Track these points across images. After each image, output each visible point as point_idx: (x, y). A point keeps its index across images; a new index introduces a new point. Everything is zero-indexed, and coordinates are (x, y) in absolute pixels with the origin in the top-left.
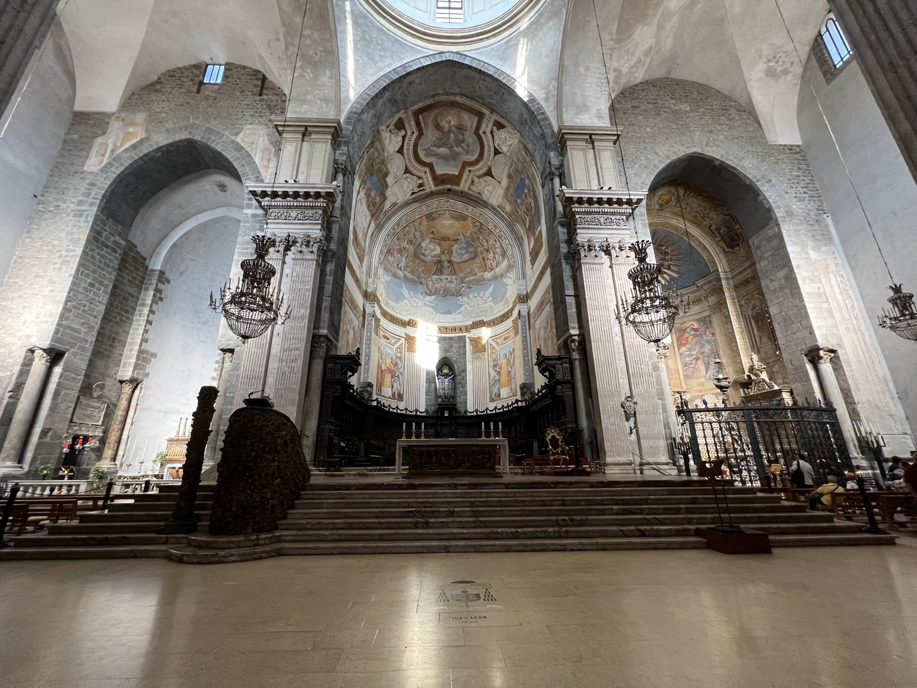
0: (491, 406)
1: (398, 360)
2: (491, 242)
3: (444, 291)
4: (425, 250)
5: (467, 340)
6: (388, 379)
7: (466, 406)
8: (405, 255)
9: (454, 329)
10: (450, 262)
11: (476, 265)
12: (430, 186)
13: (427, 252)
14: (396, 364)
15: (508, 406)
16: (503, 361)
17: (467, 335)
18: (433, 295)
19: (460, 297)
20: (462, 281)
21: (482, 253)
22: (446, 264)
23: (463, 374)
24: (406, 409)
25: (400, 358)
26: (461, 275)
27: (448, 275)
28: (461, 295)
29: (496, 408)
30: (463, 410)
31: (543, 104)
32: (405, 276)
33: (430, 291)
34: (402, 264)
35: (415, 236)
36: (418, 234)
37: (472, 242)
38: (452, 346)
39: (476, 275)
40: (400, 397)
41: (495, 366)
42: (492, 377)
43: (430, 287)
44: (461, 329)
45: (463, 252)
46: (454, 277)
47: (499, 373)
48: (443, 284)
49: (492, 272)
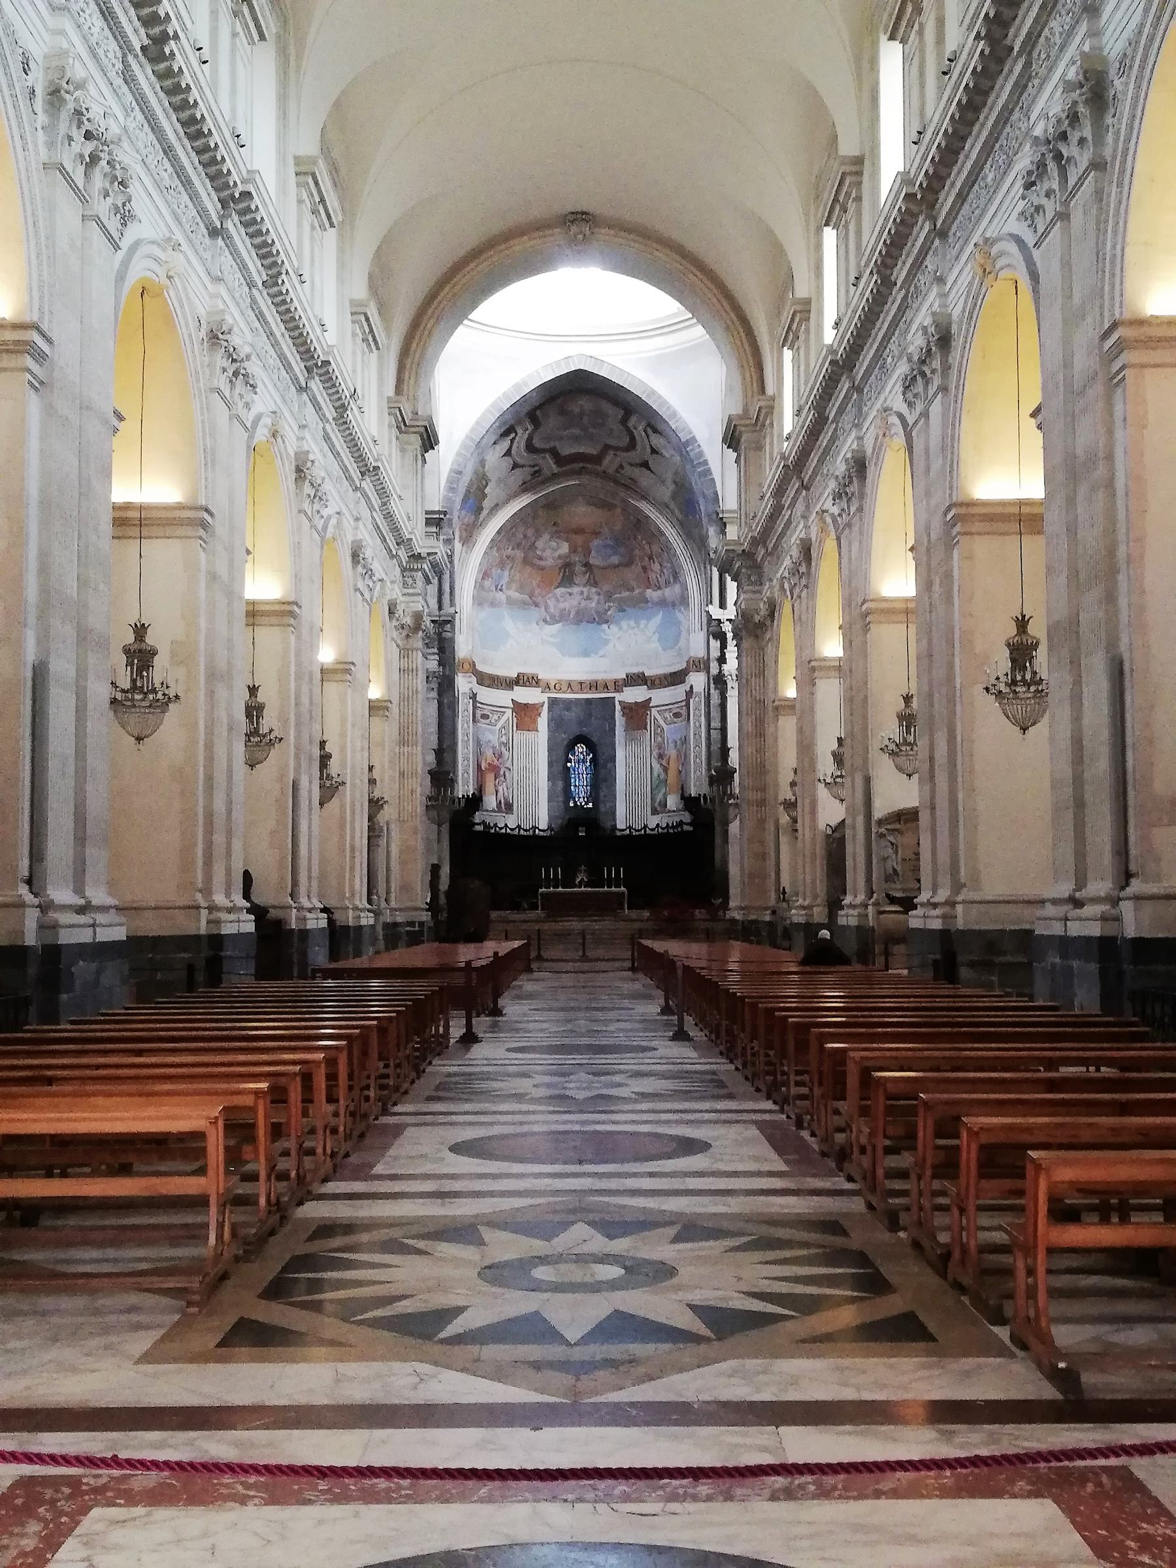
0: (653, 822)
1: (503, 750)
2: (655, 548)
3: (577, 613)
4: (544, 550)
5: (618, 707)
6: (490, 779)
7: (614, 820)
8: (508, 567)
9: (594, 686)
10: (587, 565)
11: (630, 574)
12: (549, 465)
13: (548, 553)
14: (500, 756)
15: (673, 827)
16: (672, 752)
17: (618, 697)
18: (558, 622)
19: (605, 626)
20: (609, 597)
21: (642, 559)
22: (578, 568)
23: (609, 765)
24: (519, 827)
25: (505, 745)
26: (606, 587)
27: (584, 586)
28: (607, 622)
29: (658, 825)
30: (608, 824)
31: (704, 447)
32: (508, 598)
33: (552, 617)
34: (504, 581)
35: (525, 536)
36: (530, 532)
37: (620, 541)
38: (590, 715)
39: (632, 590)
40: (509, 808)
41: (661, 756)
42: (655, 774)
43: (552, 610)
44: (606, 686)
45: (609, 551)
46: (594, 590)
47: (666, 770)
48: (575, 603)
49: (659, 592)
